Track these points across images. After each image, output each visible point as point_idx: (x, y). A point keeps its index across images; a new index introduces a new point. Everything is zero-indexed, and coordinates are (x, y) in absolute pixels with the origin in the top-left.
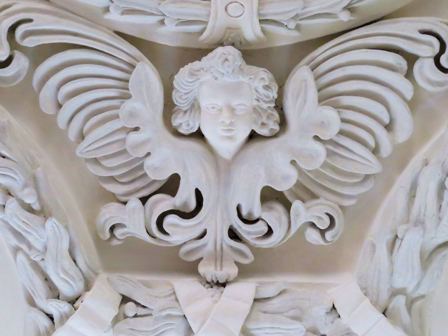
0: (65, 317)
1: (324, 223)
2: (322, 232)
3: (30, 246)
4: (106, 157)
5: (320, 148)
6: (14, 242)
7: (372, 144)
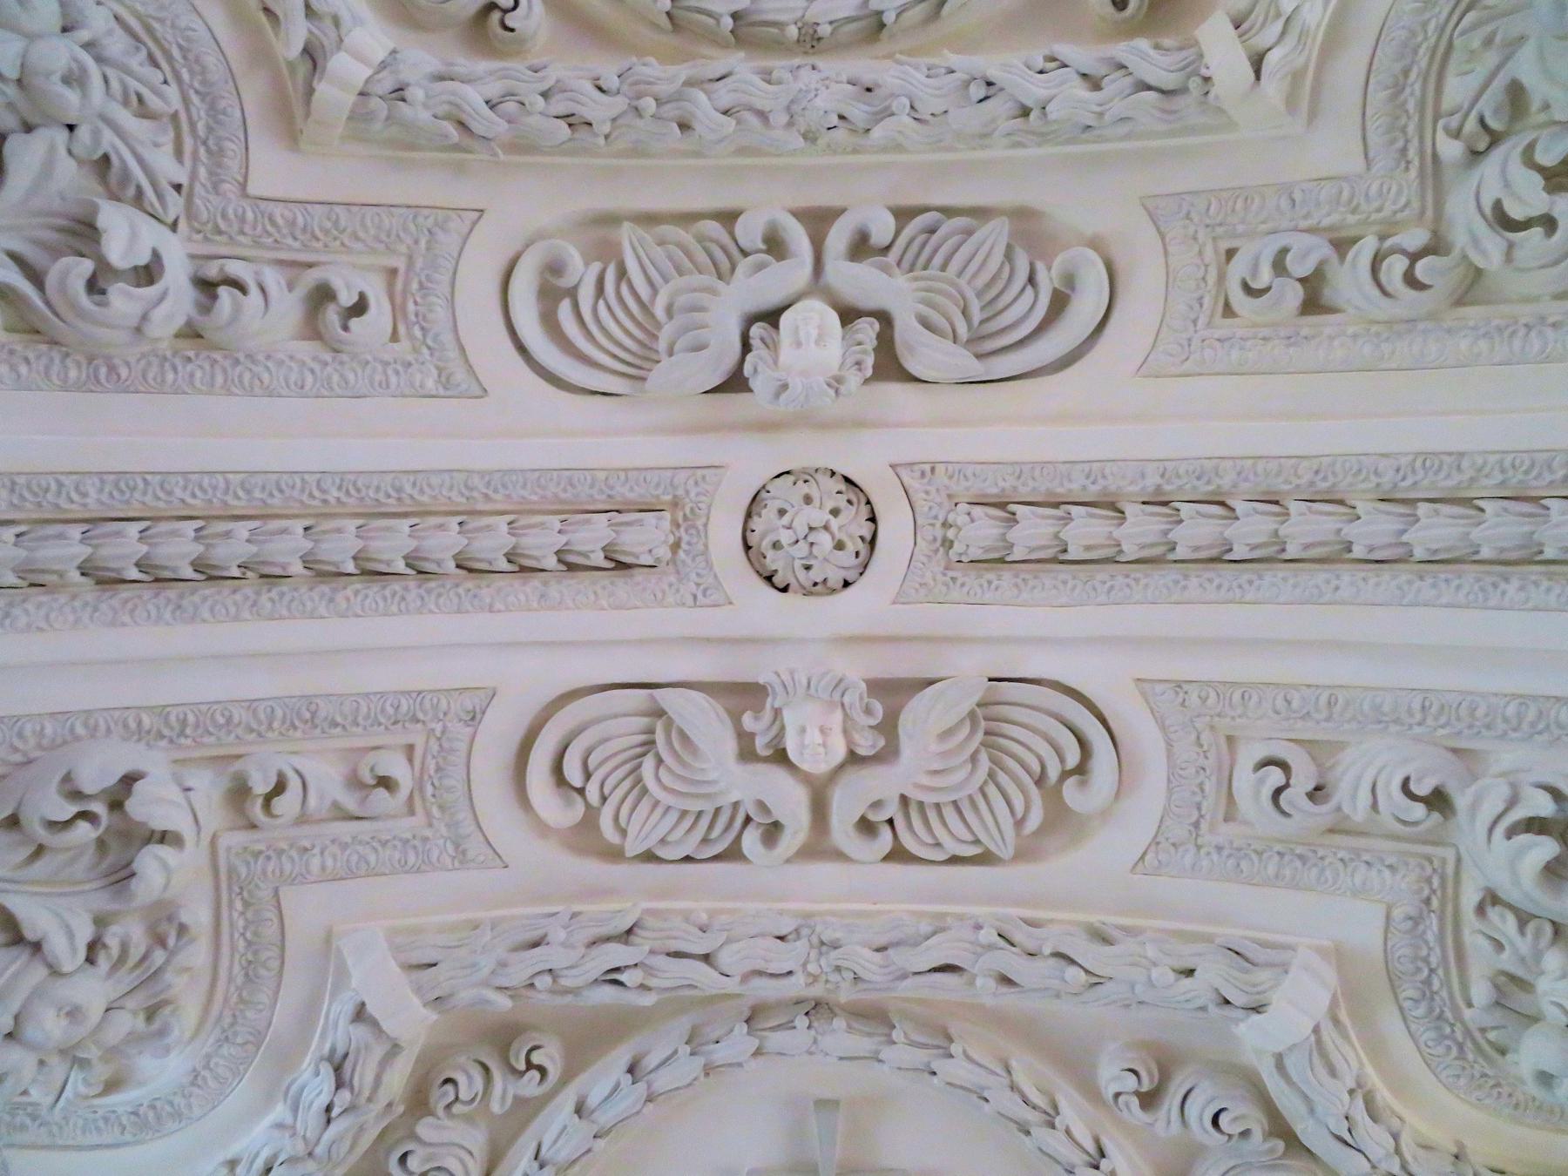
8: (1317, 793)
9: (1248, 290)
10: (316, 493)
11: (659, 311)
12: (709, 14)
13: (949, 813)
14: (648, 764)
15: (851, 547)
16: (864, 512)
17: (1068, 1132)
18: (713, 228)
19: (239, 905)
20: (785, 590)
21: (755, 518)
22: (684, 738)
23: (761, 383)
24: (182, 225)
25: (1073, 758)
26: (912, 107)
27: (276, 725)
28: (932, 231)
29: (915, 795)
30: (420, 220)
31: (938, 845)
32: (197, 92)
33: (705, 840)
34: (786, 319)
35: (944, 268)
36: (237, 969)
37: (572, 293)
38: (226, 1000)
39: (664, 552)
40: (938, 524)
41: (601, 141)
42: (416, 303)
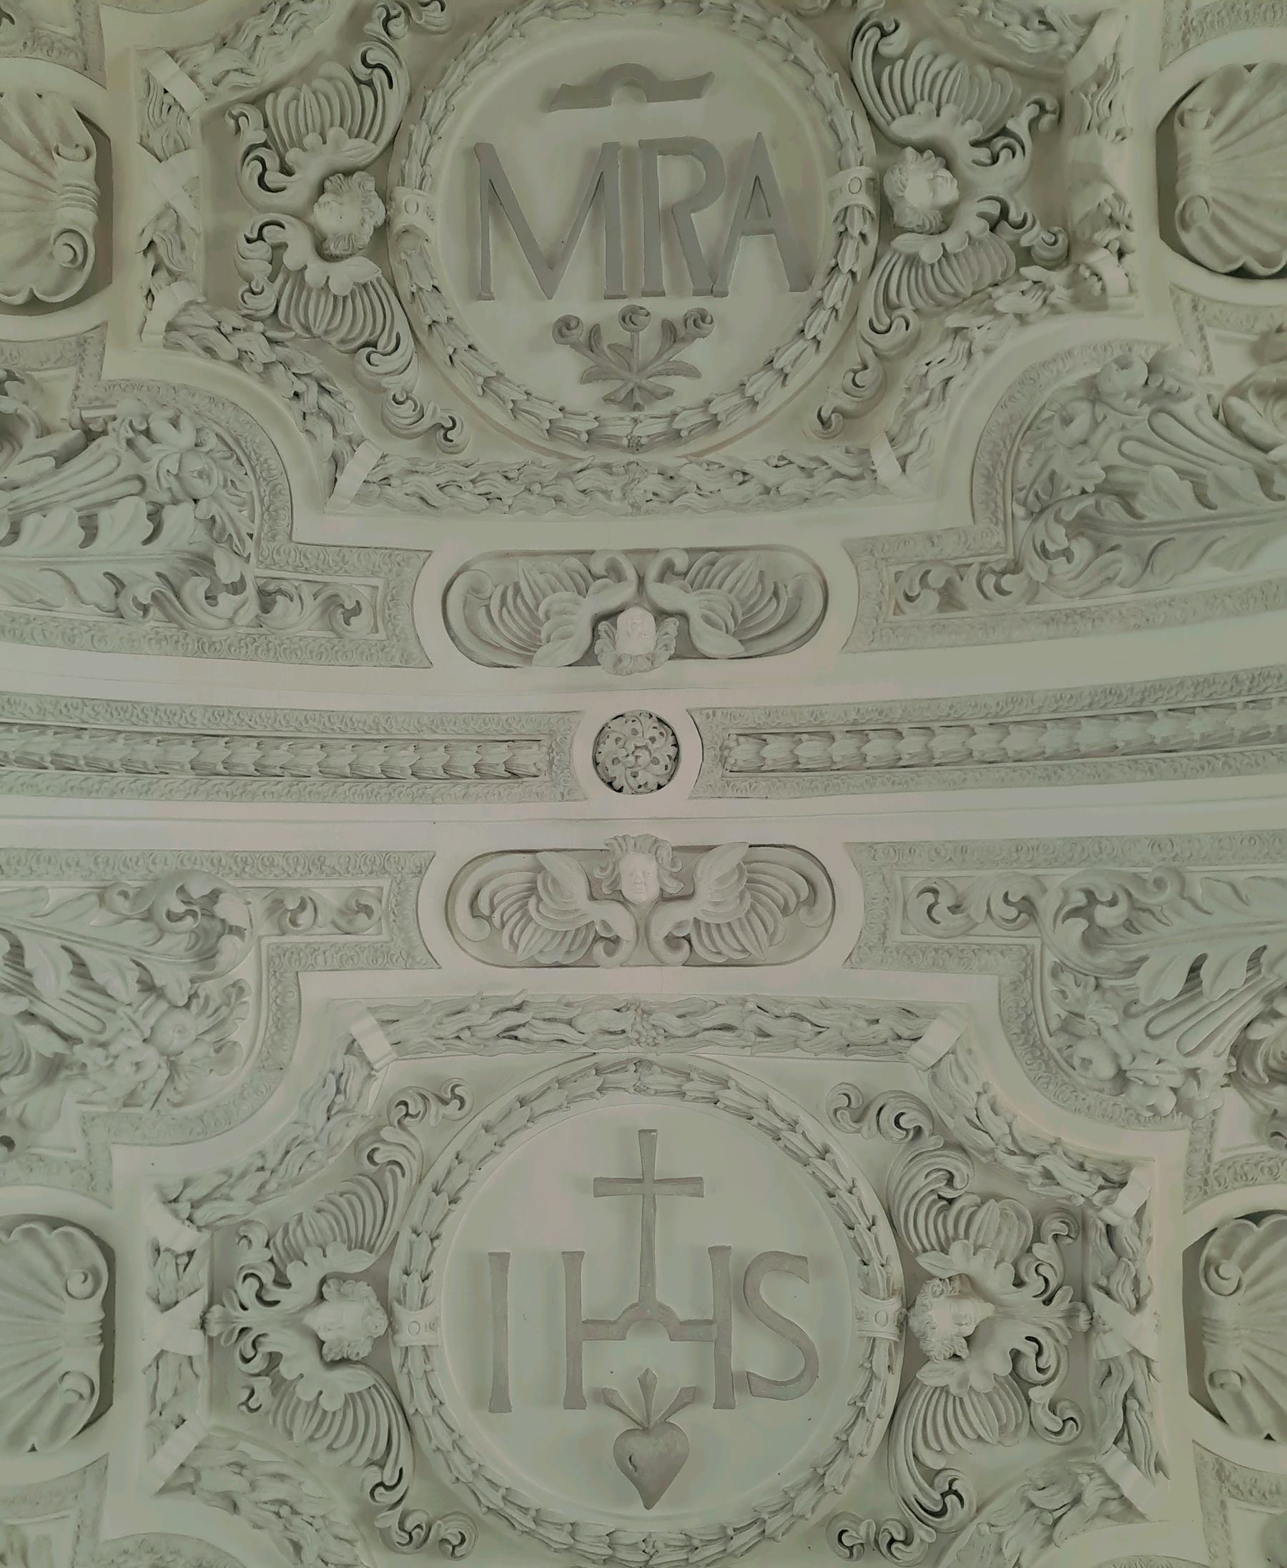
0: (176, 1214)
1: (253, 1403)
2: (246, 1403)
3: (232, 1187)
4: (303, 1230)
5: (310, 1397)
6: (236, 1173)
7: (316, 1437)
8: (955, 909)
10: (327, 724)
11: (541, 614)
12: (574, 432)
13: (725, 930)
14: (532, 902)
15: (663, 763)
16: (671, 739)
17: (803, 1133)
18: (574, 562)
19: (273, 982)
20: (620, 791)
21: (602, 745)
22: (554, 881)
23: (606, 658)
24: (253, 559)
25: (805, 891)
27: (299, 869)
28: (713, 564)
29: (704, 919)
30: (393, 557)
31: (719, 953)
33: (568, 952)
34: (621, 619)
35: (720, 587)
36: (271, 1023)
38: (264, 1042)
39: (544, 767)
40: (717, 748)
42: (389, 609)
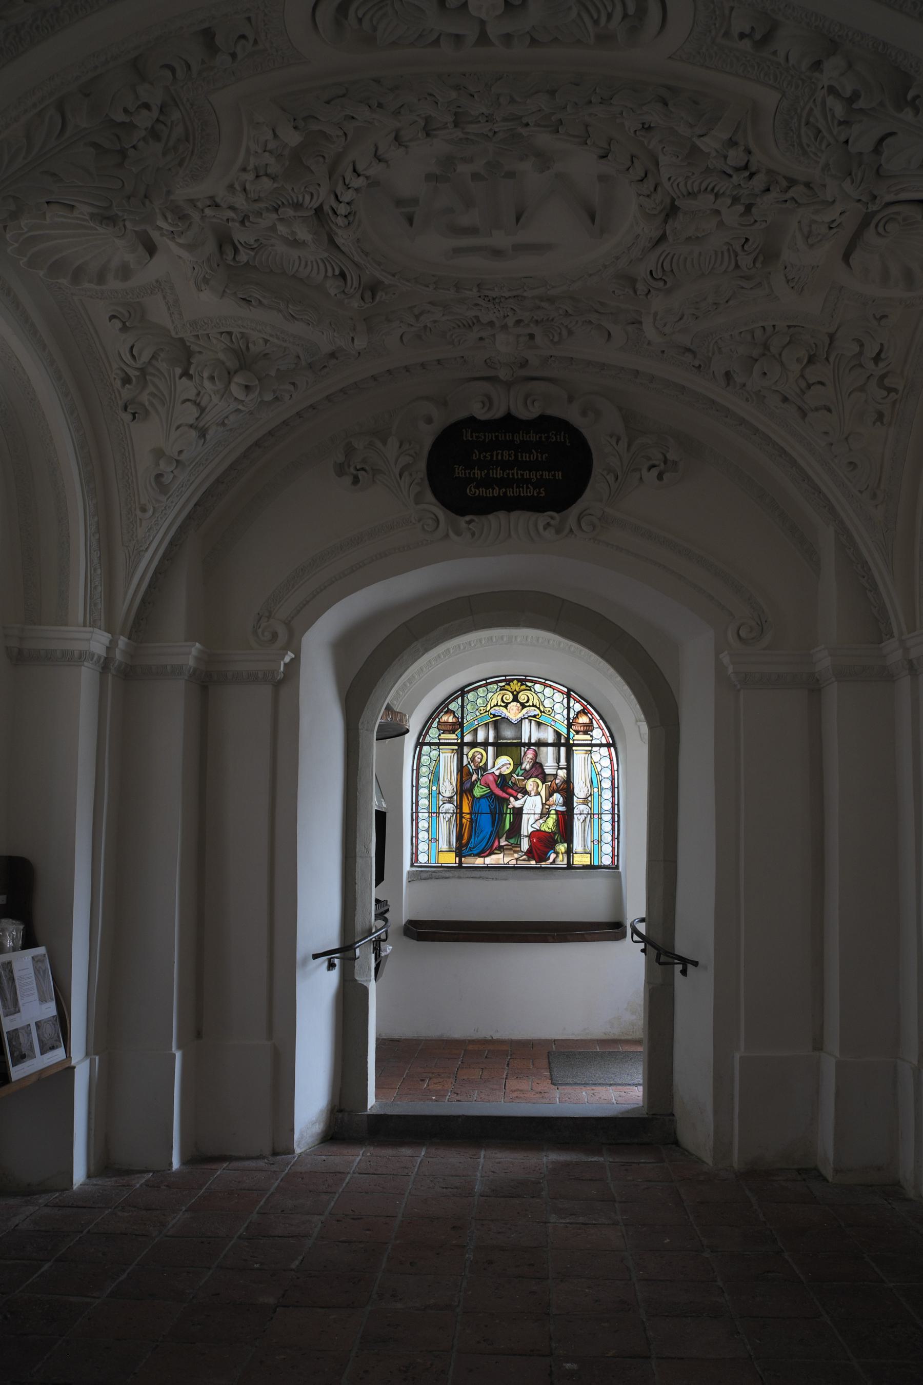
9: (243, 37)
26: (437, 103)
32: (792, 130)
37: (625, 16)
41: (598, 90)
42: (715, 24)
